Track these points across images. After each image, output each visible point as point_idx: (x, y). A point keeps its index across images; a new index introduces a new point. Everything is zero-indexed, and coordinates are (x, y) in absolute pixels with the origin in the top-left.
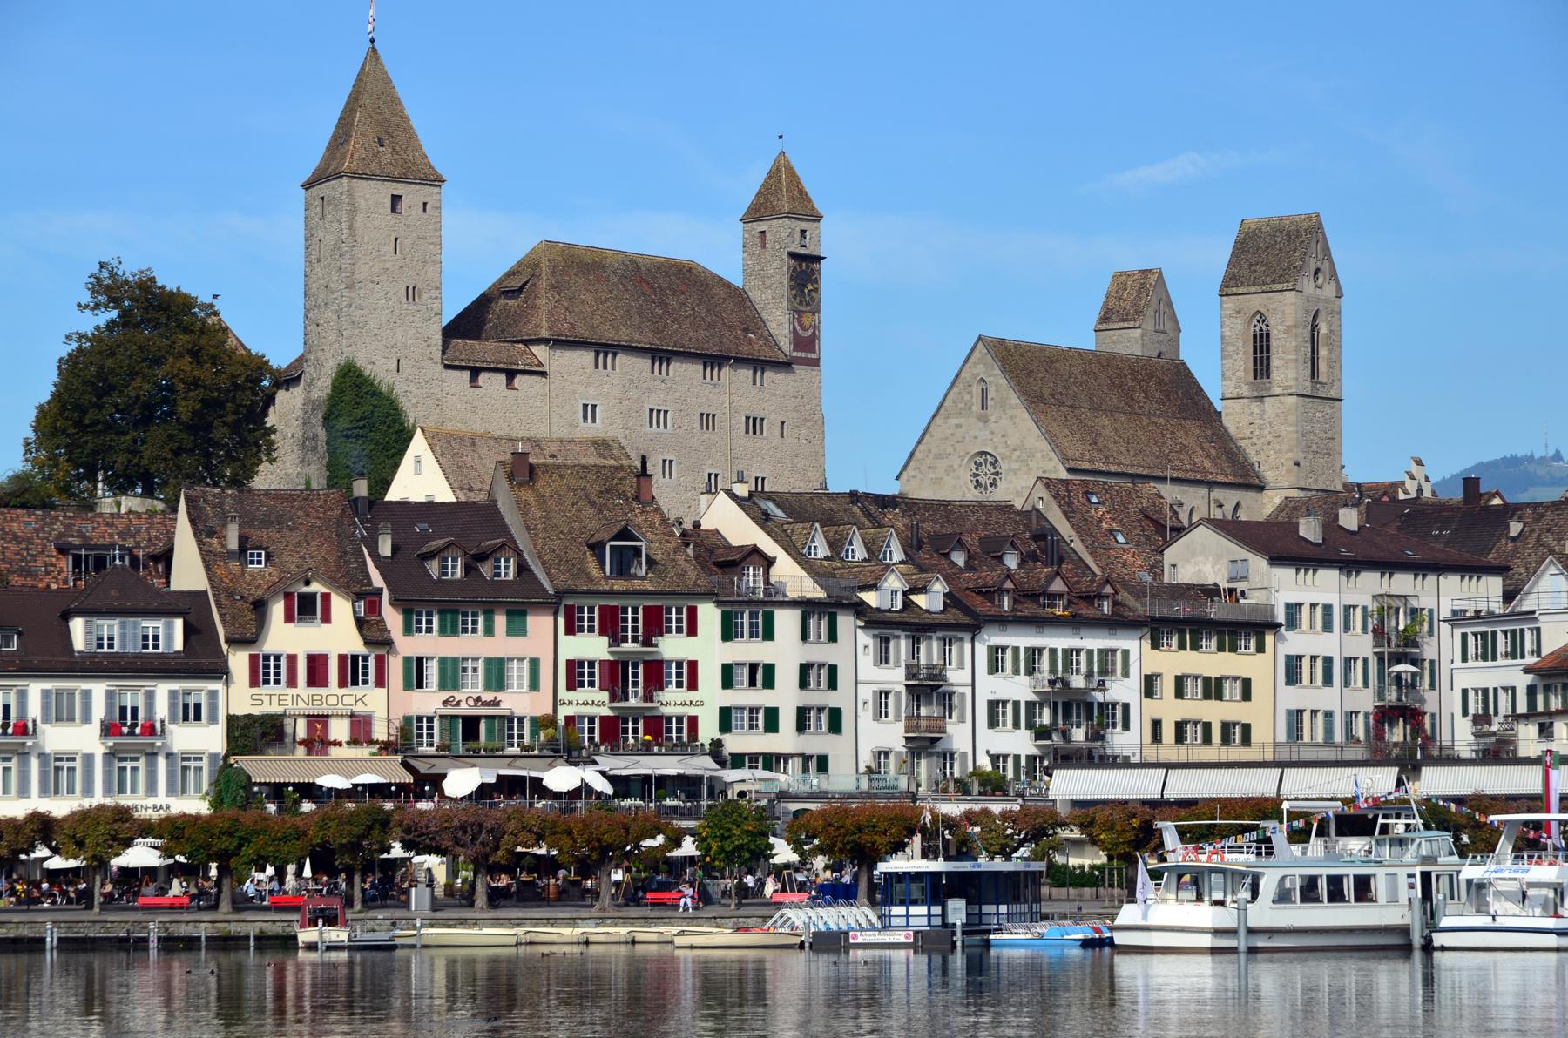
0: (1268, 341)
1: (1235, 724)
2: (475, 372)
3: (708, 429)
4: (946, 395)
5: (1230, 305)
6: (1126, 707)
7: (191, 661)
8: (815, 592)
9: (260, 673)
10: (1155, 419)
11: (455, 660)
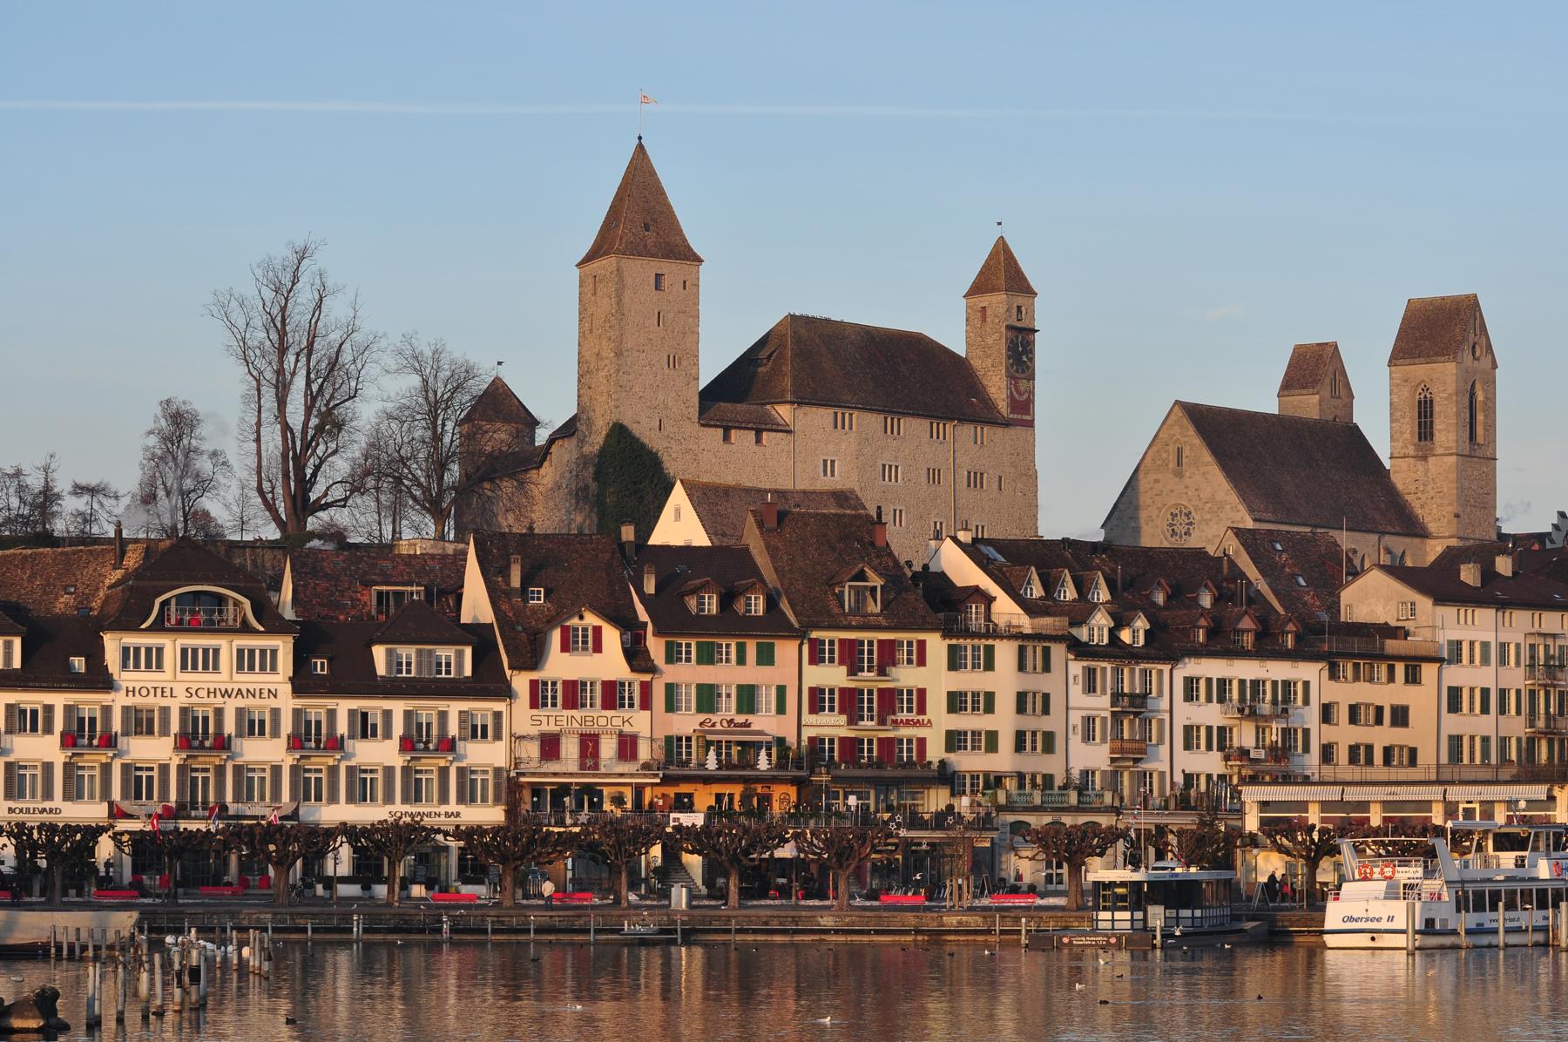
0: (1431, 407)
4: (1146, 453)
5: (1398, 375)
6: (1306, 732)
9: (538, 696)
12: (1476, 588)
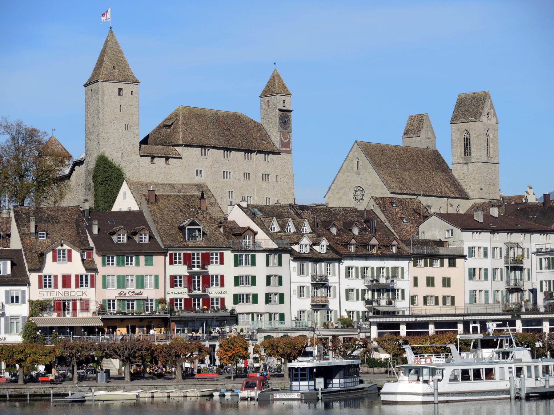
1: (448, 297)
2: (153, 158)
3: (247, 179)
5: (454, 127)
6: (403, 291)
7: (14, 279)
8: (272, 245)
9: (44, 282)
10: (426, 173)
11: (124, 276)
12: (481, 223)
